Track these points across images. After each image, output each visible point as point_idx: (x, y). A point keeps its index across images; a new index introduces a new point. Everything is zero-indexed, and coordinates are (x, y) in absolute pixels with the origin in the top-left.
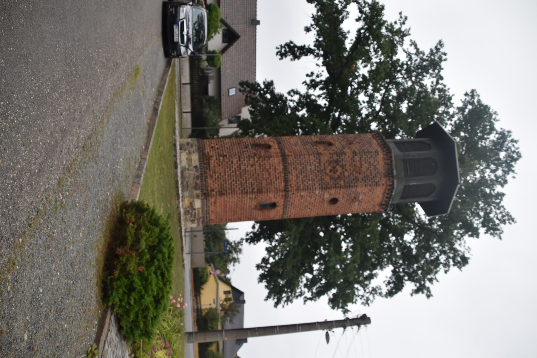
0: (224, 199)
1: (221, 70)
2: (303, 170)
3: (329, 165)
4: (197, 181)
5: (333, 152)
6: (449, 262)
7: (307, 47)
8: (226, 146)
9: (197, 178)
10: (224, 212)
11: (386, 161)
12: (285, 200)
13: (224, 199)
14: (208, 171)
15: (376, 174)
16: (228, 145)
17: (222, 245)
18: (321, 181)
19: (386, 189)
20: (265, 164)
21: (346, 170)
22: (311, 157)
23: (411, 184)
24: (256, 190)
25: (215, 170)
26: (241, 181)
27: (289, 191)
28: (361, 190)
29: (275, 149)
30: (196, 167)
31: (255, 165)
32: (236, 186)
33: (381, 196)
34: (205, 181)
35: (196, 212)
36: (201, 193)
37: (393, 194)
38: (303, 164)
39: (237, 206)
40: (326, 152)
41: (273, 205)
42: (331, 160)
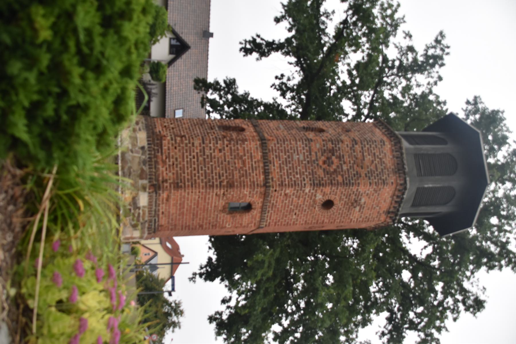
0: (181, 195)
1: (167, 86)
2: (288, 160)
3: (322, 155)
4: (144, 167)
5: (327, 139)
6: (458, 308)
7: (277, 42)
8: (184, 126)
9: (144, 162)
10: (179, 215)
11: (395, 153)
12: (264, 199)
13: (181, 195)
14: (160, 154)
15: (382, 170)
16: (187, 125)
17: (160, 306)
18: (313, 175)
19: (396, 189)
20: (238, 149)
21: (345, 163)
22: (298, 143)
23: (426, 186)
24: (225, 183)
25: (169, 153)
26: (205, 171)
27: (269, 186)
28: (364, 189)
29: (251, 132)
30: (143, 148)
31: (224, 150)
32: (199, 177)
33: (389, 200)
34: (155, 168)
35: (141, 212)
36: (148, 185)
37: (405, 196)
38: (288, 152)
39: (198, 207)
40: (317, 138)
41: (248, 208)
42: (325, 148)
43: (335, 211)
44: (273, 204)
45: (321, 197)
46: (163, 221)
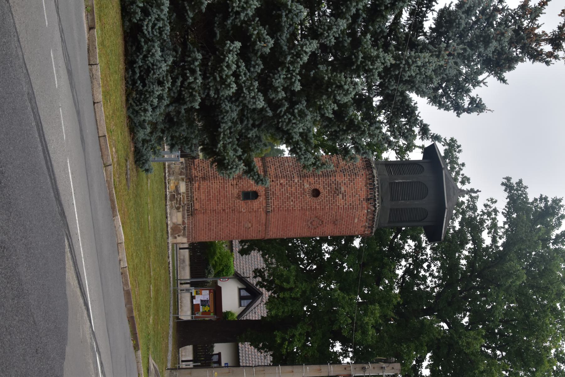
9: (183, 168)
23: (397, 181)
33: (364, 189)
37: (376, 182)
43: (323, 198)
44: (273, 192)
45: (308, 186)
46: (197, 206)
